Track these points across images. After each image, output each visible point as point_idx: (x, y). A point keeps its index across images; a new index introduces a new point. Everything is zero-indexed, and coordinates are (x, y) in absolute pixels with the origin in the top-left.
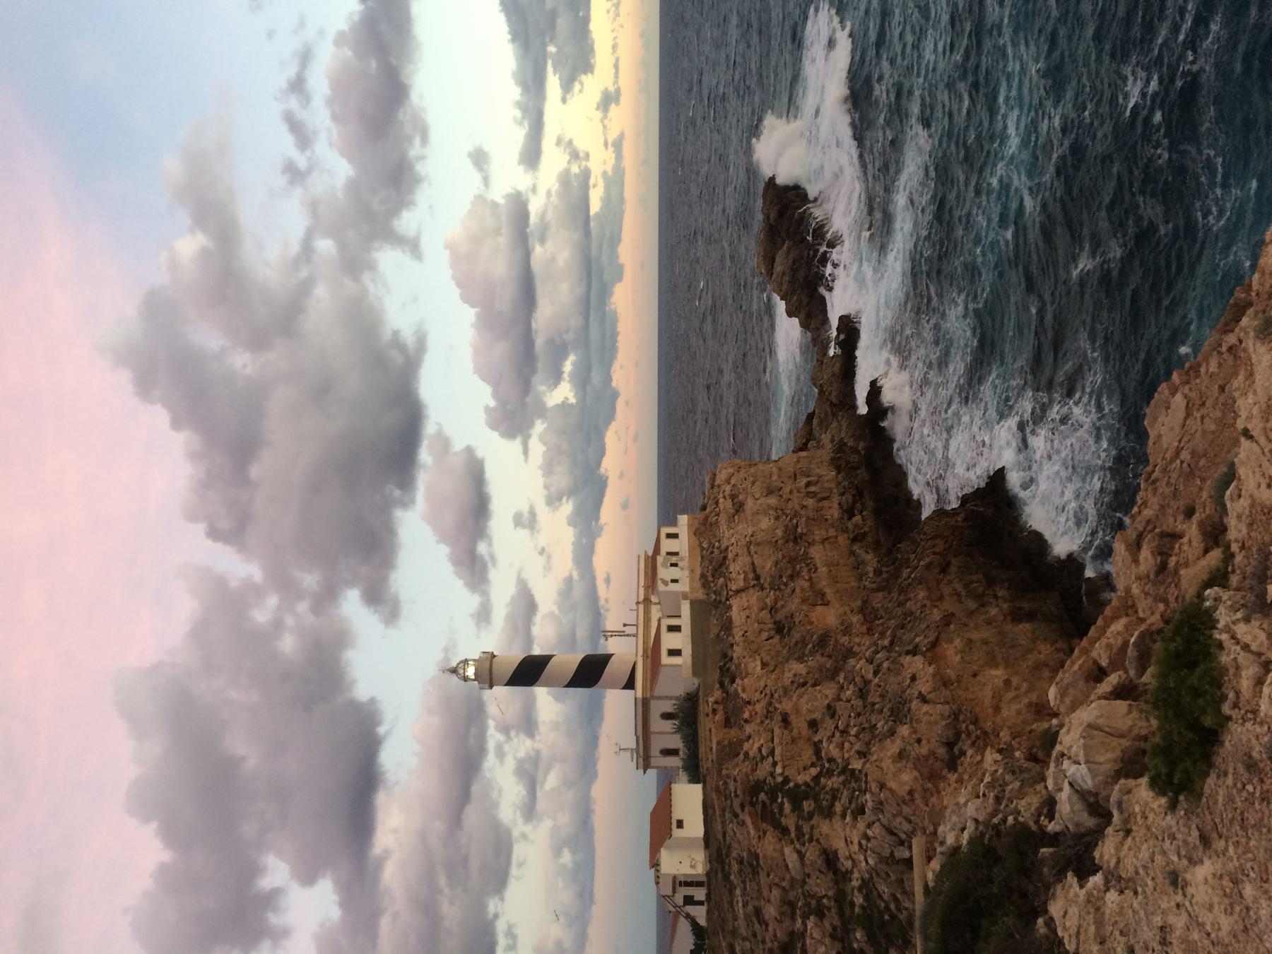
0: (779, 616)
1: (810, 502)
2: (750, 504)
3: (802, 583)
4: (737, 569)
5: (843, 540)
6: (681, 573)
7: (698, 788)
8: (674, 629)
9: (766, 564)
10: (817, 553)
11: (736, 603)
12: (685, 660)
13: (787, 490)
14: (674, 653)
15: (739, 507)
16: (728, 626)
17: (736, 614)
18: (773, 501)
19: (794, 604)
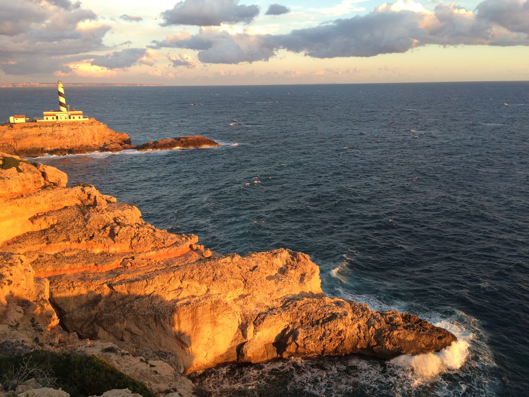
0: (43, 135)
1: (69, 140)
2: (72, 131)
3: (48, 138)
4: (57, 129)
5: (61, 145)
6: (63, 119)
8: (53, 118)
9: (56, 133)
10: (57, 141)
11: (51, 128)
12: (45, 120)
13: (73, 137)
14: (47, 119)
15: (73, 129)
16: (46, 126)
17: (48, 128)
19: (43, 136)
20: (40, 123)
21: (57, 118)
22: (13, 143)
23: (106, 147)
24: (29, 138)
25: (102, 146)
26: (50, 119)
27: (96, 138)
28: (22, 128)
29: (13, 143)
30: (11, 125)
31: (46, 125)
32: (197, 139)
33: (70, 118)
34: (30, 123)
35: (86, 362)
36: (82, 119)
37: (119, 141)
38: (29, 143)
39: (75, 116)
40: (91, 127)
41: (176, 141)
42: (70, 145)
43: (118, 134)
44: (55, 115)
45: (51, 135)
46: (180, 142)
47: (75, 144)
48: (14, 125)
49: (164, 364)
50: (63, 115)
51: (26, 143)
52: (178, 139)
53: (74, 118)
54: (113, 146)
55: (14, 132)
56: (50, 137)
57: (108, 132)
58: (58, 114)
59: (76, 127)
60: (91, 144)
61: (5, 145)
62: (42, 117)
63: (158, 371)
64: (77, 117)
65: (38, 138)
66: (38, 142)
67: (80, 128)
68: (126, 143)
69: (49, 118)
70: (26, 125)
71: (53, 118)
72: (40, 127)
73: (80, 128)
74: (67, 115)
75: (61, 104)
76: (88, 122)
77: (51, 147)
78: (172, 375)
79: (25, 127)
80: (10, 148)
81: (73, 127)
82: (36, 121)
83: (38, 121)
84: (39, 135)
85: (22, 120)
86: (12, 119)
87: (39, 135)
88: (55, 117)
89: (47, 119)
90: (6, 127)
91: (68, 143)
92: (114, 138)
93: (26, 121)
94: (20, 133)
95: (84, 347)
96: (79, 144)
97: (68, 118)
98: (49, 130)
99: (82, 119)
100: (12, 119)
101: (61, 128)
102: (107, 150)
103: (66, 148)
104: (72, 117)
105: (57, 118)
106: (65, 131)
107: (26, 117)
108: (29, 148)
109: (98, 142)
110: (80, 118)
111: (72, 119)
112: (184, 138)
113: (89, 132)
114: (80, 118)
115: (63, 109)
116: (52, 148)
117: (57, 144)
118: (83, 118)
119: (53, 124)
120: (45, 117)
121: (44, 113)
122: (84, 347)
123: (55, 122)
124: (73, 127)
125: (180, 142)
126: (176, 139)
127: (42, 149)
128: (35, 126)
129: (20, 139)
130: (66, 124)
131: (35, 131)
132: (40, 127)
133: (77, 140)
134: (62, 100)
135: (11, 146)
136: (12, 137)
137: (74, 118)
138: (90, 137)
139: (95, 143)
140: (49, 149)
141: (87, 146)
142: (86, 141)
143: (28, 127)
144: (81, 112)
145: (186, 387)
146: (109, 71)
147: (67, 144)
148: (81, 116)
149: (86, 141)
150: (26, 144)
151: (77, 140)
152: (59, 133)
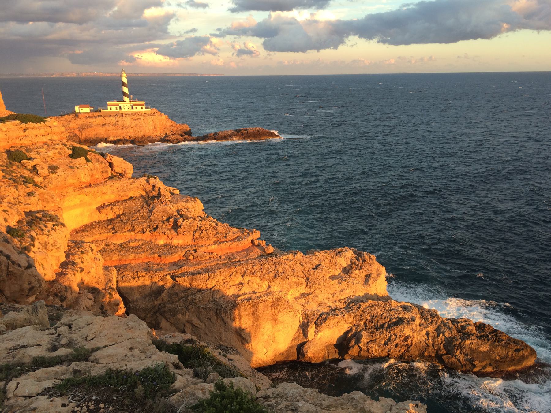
0: (107, 125)
1: (131, 131)
2: (135, 121)
3: (111, 128)
4: (120, 119)
6: (126, 110)
7: (89, 111)
8: (117, 109)
9: (119, 123)
10: (120, 131)
11: (114, 118)
12: (109, 110)
13: (136, 128)
14: (111, 109)
16: (110, 116)
17: (112, 118)
18: (134, 125)
19: (107, 126)
20: (104, 113)
21: (120, 108)
22: (78, 133)
23: (167, 138)
24: (93, 128)
25: (163, 137)
26: (114, 109)
27: (158, 129)
28: (87, 118)
29: (78, 133)
30: (77, 115)
31: (110, 115)
32: (258, 131)
33: (133, 108)
34: (94, 113)
35: (196, 353)
36: (144, 110)
37: (179, 132)
38: (93, 133)
39: (138, 107)
40: (152, 118)
41: (236, 133)
42: (132, 135)
43: (178, 125)
44: (118, 105)
45: (114, 125)
46: (240, 134)
47: (137, 135)
48: (79, 115)
49: (241, 358)
50: (126, 105)
51: (90, 133)
52: (239, 131)
53: (136, 108)
54: (174, 137)
55: (80, 122)
56: (114, 128)
57: (169, 123)
58: (121, 104)
59: (138, 117)
60: (152, 135)
61: (71, 134)
62: (107, 105)
63: (236, 364)
64: (139, 107)
65: (102, 128)
66: (101, 132)
67: (142, 118)
68: (187, 135)
69: (112, 108)
70: (91, 114)
71: (117, 109)
72: (104, 117)
73: (142, 118)
74: (130, 106)
75: (124, 94)
76: (150, 113)
77: (114, 137)
78: (250, 370)
79: (89, 117)
80: (76, 138)
81: (135, 117)
82: (100, 111)
83: (102, 110)
84: (104, 125)
85: (87, 110)
86: (77, 109)
87: (104, 125)
88: (118, 107)
89: (111, 109)
90: (71, 116)
91: (130, 133)
92: (175, 129)
93: (91, 111)
94: (85, 122)
95: (164, 337)
96: (141, 134)
97: (131, 108)
98: (113, 120)
99: (144, 110)
100: (77, 109)
101: (124, 119)
102: (168, 141)
103: (128, 138)
104: (134, 107)
105: (120, 108)
106: (128, 121)
107: (91, 107)
108: (93, 137)
109: (160, 133)
110: (142, 108)
111: (134, 110)
112: (244, 130)
113: (150, 122)
114: (142, 108)
115: (126, 99)
116: (116, 139)
117: (120, 134)
118: (146, 108)
119: (116, 115)
120: (109, 107)
121: (109, 103)
122: (164, 337)
123: (118, 112)
124: (135, 117)
125: (240, 134)
126: (236, 130)
127: (106, 139)
128: (99, 116)
129: (84, 129)
130: (129, 114)
131: (99, 121)
132: (104, 117)
133: (139, 130)
134: (126, 90)
135: (76, 135)
136: (77, 127)
137: (136, 108)
138: (151, 128)
139: (156, 134)
140: (112, 139)
141: (149, 137)
142: (148, 131)
143: (92, 117)
144: (144, 102)
145: (264, 383)
146: (172, 61)
147: (129, 134)
148: (144, 107)
149: (148, 131)
150: (90, 133)
151: (139, 130)
152: (122, 123)
